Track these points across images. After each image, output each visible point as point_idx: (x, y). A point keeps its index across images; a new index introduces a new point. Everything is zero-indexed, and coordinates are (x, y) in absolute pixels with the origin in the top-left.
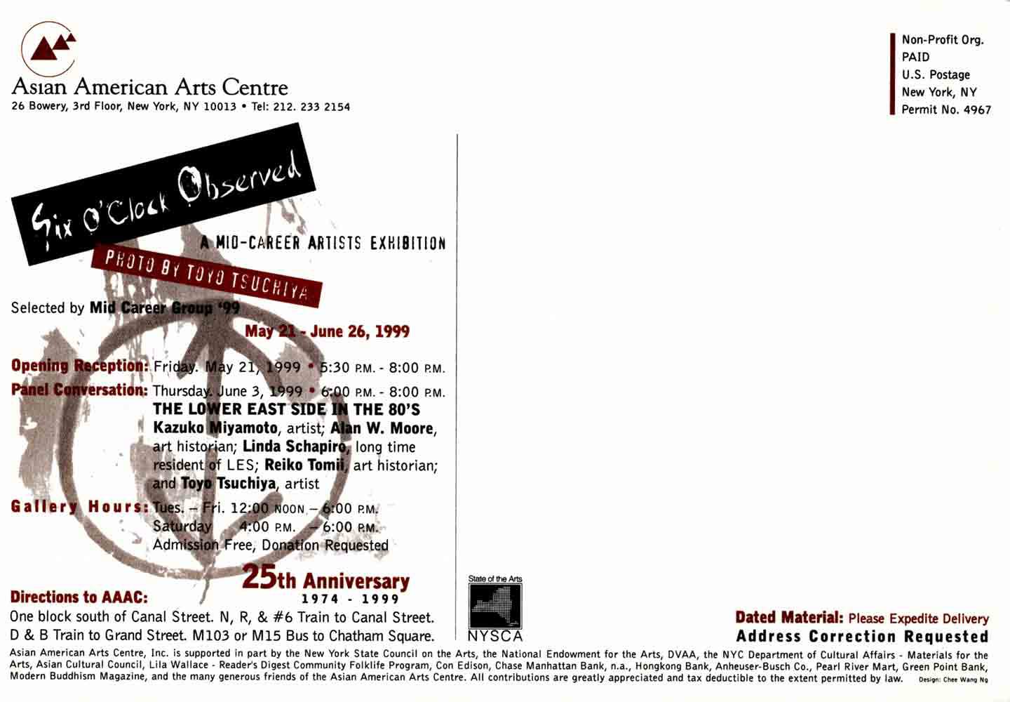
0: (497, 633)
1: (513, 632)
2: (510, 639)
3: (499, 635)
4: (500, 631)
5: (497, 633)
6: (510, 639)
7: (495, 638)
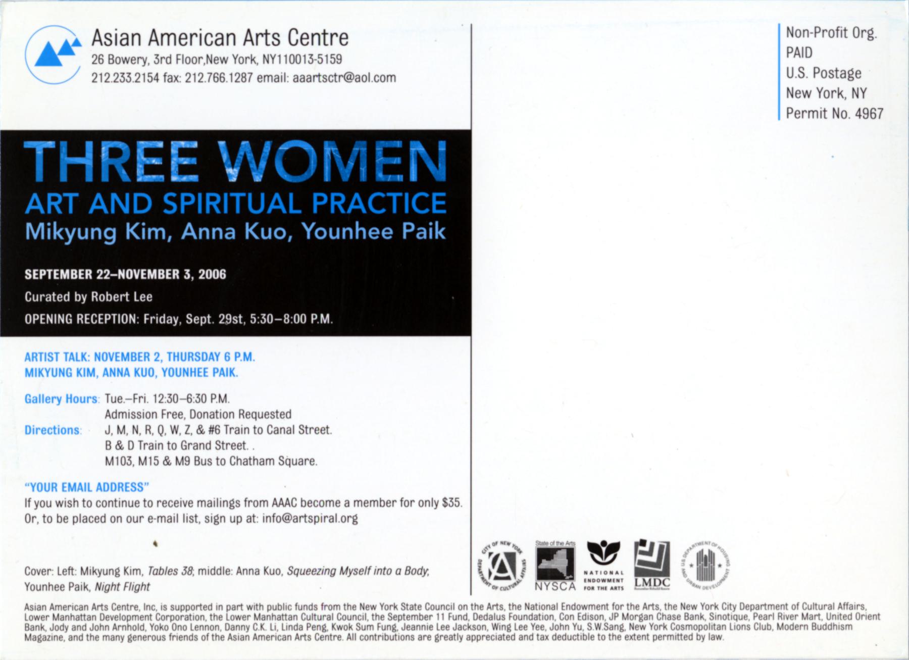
0: (557, 584)
1: (569, 583)
2: (566, 589)
3: (559, 586)
4: (559, 582)
5: (557, 584)
6: (566, 589)
7: (555, 588)
